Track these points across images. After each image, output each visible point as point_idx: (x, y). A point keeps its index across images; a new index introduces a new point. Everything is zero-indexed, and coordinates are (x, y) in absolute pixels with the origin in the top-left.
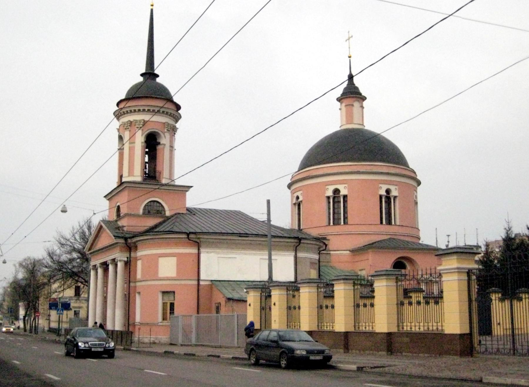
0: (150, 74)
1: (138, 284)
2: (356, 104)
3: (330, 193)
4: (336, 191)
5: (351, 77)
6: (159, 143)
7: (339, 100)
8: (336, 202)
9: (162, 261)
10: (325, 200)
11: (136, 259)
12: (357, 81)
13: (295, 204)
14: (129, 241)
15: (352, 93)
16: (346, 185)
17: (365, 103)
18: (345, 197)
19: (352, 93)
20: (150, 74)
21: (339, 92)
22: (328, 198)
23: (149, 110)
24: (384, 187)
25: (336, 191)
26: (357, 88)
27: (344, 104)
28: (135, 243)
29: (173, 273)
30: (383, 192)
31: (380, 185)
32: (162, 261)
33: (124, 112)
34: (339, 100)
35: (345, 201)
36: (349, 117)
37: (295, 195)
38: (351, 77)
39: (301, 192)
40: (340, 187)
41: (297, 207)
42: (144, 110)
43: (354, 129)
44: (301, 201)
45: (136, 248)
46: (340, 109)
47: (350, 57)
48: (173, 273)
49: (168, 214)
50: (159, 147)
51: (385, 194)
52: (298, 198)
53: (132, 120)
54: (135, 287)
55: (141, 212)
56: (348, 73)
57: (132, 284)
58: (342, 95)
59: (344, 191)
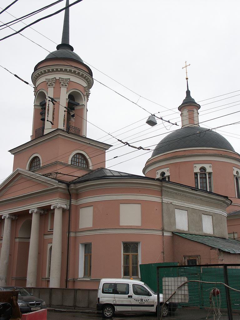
0: (65, 45)
1: (79, 234)
2: (195, 110)
3: (197, 170)
4: (203, 169)
5: (188, 92)
6: (78, 105)
8: (203, 177)
9: (123, 207)
11: (78, 208)
12: (192, 95)
14: (72, 186)
15: (189, 105)
16: (211, 165)
19: (189, 105)
20: (65, 45)
21: (181, 103)
22: (196, 174)
23: (75, 72)
25: (203, 169)
28: (77, 190)
29: (137, 222)
32: (123, 207)
33: (41, 72)
34: (180, 108)
35: (209, 178)
38: (188, 92)
42: (70, 71)
45: (78, 196)
47: (187, 79)
48: (137, 222)
49: (91, 168)
50: (77, 108)
53: (57, 78)
54: (75, 238)
55: (70, 163)
57: (72, 235)
59: (209, 169)
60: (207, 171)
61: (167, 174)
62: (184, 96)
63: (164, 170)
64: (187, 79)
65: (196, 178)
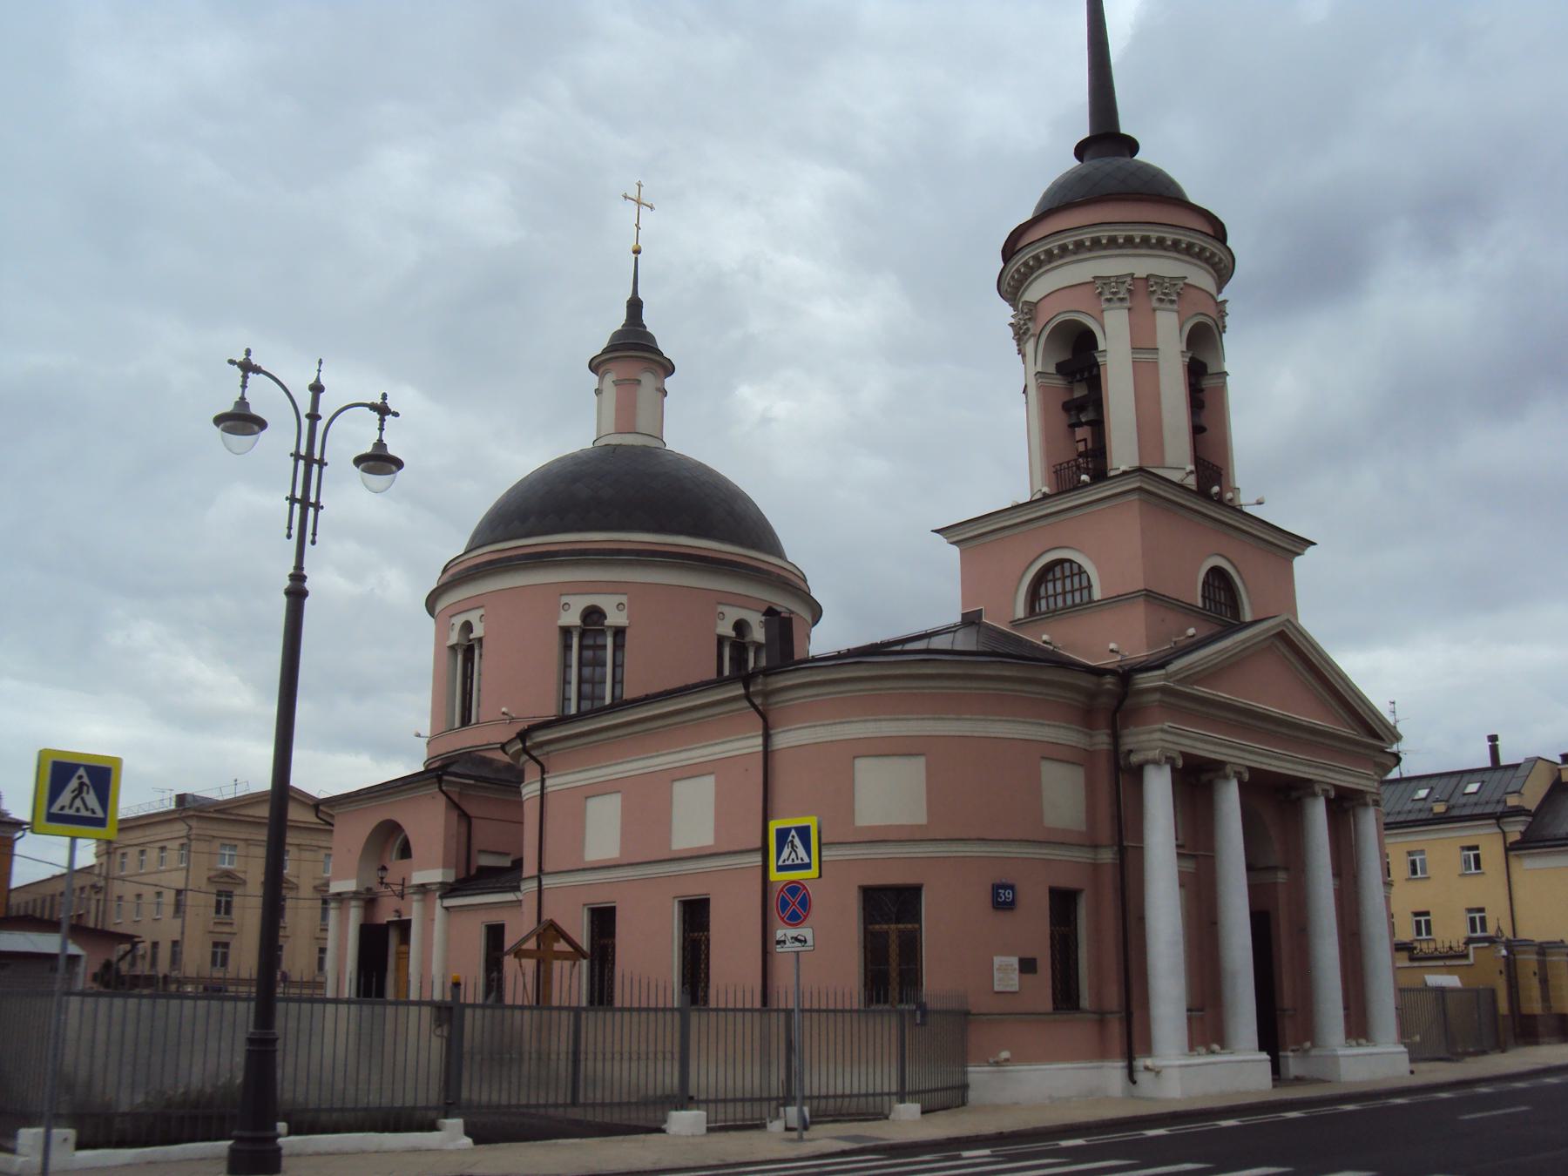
2: (648, 380)
3: (572, 618)
4: (593, 615)
5: (635, 306)
7: (595, 365)
10: (555, 640)
12: (647, 318)
13: (453, 648)
15: (634, 351)
16: (624, 599)
17: (669, 383)
18: (619, 632)
19: (634, 351)
21: (599, 342)
22: (566, 632)
24: (733, 614)
25: (593, 615)
26: (651, 338)
27: (610, 378)
30: (726, 629)
31: (721, 608)
34: (595, 365)
35: (619, 646)
36: (626, 416)
37: (458, 621)
38: (635, 306)
39: (481, 612)
40: (607, 603)
41: (460, 658)
43: (633, 446)
44: (480, 640)
46: (598, 392)
47: (637, 252)
51: (733, 634)
52: (467, 627)
56: (629, 295)
58: (605, 351)
59: (615, 618)
60: (607, 622)
61: (478, 632)
62: (619, 319)
63: (473, 617)
64: (637, 252)
65: (567, 647)
